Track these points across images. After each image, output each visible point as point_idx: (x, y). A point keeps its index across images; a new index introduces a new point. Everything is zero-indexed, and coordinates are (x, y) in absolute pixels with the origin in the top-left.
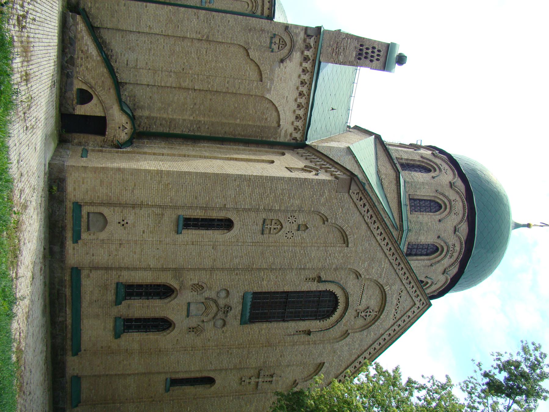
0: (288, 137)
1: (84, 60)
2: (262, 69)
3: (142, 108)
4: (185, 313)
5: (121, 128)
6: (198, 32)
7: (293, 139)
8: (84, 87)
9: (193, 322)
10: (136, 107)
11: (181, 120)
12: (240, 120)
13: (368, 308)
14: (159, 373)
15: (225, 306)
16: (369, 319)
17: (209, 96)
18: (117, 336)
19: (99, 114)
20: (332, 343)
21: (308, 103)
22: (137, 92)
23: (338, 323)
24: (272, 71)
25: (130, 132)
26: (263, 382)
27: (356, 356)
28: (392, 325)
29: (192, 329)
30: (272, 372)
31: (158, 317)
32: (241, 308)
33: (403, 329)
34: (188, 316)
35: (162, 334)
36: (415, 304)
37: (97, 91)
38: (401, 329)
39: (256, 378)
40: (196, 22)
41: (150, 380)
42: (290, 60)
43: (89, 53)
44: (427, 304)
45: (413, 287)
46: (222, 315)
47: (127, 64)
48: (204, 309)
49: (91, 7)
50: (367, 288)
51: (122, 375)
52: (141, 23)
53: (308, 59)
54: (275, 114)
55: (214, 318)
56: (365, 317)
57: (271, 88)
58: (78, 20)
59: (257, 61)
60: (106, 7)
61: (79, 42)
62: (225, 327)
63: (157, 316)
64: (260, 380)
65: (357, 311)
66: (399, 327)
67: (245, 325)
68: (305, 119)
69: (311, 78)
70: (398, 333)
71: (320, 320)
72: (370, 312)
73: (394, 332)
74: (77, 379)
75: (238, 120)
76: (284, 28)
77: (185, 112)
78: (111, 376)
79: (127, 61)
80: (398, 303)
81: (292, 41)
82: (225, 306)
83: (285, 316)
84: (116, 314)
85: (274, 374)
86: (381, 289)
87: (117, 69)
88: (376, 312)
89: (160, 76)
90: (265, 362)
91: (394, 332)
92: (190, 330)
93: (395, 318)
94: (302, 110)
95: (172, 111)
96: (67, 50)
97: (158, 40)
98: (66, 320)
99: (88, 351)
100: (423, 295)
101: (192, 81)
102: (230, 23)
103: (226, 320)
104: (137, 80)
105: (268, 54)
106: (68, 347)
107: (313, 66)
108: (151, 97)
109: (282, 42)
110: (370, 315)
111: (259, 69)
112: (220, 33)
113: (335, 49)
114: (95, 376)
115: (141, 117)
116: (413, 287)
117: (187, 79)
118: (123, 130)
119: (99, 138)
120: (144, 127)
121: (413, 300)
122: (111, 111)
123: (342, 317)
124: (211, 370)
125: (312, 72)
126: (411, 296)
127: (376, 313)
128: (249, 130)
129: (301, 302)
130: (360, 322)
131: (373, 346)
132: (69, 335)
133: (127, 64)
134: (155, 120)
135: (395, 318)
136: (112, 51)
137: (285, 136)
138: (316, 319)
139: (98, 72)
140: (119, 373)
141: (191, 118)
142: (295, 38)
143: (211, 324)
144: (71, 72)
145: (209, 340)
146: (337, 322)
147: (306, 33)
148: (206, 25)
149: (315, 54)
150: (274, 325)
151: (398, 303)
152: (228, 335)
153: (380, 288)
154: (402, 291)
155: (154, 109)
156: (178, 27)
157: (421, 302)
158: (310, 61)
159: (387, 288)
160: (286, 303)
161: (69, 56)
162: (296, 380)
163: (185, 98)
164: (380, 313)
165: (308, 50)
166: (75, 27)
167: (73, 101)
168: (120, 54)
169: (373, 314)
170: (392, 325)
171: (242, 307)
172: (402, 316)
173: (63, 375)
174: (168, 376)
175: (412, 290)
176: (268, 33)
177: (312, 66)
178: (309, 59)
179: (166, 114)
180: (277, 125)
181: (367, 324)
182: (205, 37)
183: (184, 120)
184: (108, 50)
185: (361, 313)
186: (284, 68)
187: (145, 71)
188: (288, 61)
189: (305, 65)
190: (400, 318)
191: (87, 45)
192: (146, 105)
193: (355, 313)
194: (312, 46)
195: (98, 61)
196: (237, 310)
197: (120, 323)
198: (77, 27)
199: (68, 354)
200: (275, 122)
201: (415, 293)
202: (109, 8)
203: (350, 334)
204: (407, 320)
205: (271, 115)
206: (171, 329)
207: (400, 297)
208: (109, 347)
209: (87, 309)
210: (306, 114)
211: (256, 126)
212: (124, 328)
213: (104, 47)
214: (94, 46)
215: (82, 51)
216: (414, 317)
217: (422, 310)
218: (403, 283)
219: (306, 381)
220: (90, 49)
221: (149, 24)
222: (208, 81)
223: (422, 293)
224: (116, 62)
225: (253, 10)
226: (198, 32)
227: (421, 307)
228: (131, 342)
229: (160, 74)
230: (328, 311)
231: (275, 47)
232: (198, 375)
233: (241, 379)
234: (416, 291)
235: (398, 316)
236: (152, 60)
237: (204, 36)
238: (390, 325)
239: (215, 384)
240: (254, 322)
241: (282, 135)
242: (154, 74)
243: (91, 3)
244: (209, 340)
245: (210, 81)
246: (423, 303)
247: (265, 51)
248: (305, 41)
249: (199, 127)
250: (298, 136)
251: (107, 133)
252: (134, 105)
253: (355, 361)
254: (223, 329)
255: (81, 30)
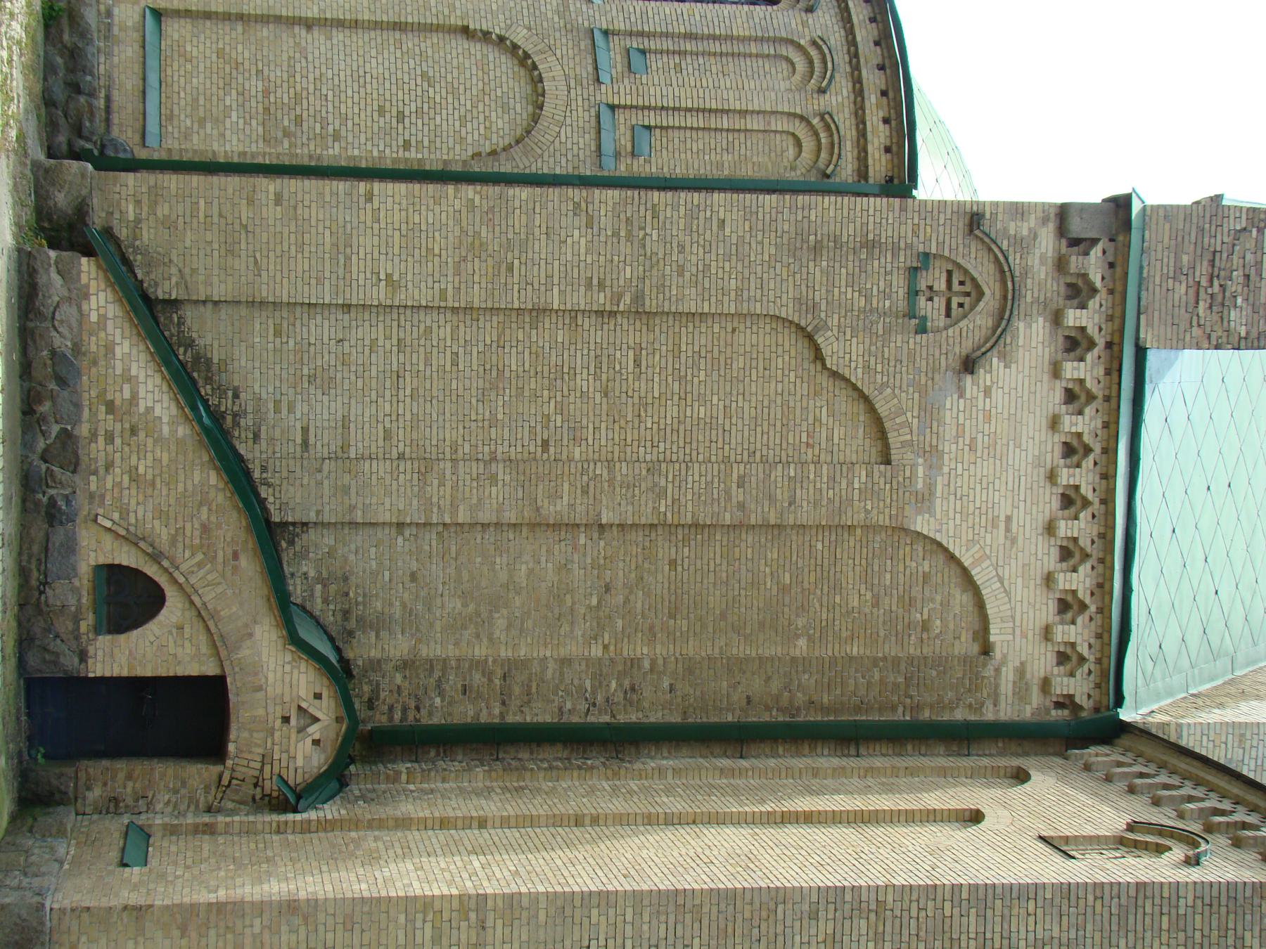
0: (1036, 698)
1: (118, 441)
2: (882, 409)
3: (380, 624)
5: (293, 721)
6: (595, 282)
7: (1059, 705)
8: (127, 557)
10: (352, 624)
11: (551, 665)
12: (810, 639)
17: (665, 550)
19: (193, 670)
21: (1106, 537)
22: (352, 557)
24: (930, 412)
25: (332, 735)
37: (184, 567)
40: (583, 241)
42: (1003, 356)
43: (142, 409)
47: (305, 443)
49: (138, 221)
52: (354, 269)
53: (1084, 344)
54: (961, 599)
57: (931, 487)
58: (84, 279)
59: (857, 377)
60: (202, 215)
61: (94, 370)
68: (1104, 610)
69: (1110, 426)
75: (802, 642)
76: (962, 224)
77: (566, 628)
79: (305, 430)
81: (1003, 272)
87: (264, 469)
89: (449, 484)
94: (1084, 569)
95: (509, 626)
96: (45, 407)
97: (429, 330)
101: (585, 492)
102: (728, 230)
104: (352, 508)
105: (903, 342)
107: (1114, 370)
108: (413, 577)
109: (961, 283)
111: (871, 409)
112: (687, 275)
113: (1204, 283)
115: (376, 665)
117: (566, 486)
118: (301, 730)
119: (198, 774)
120: (391, 708)
122: (245, 652)
125: (1112, 399)
128: (852, 682)
133: (305, 443)
134: (437, 674)
136: (236, 396)
137: (1021, 690)
139: (181, 487)
141: (596, 651)
142: (1015, 260)
144: (68, 502)
147: (1062, 231)
148: (625, 248)
149: (1116, 318)
155: (432, 625)
156: (510, 268)
158: (1096, 351)
161: (55, 429)
163: (564, 567)
165: (1083, 306)
166: (74, 310)
167: (77, 620)
168: (271, 406)
176: (895, 250)
177: (1108, 372)
178: (1092, 344)
179: (485, 640)
180: (975, 648)
182: (627, 299)
183: (565, 662)
184: (221, 390)
186: (981, 395)
187: (383, 468)
188: (995, 360)
189: (1072, 370)
191: (128, 378)
192: (397, 611)
194: (1098, 284)
195: (180, 442)
198: (85, 307)
200: (966, 637)
202: (216, 219)
205: (946, 604)
210: (1103, 587)
211: (885, 658)
213: (201, 383)
214: (158, 380)
215: (111, 407)
220: (142, 394)
221: (385, 267)
222: (655, 485)
224: (256, 437)
225: (821, 164)
226: (595, 282)
229: (448, 472)
231: (932, 310)
236: (408, 417)
237: (620, 296)
241: (1003, 689)
242: (423, 475)
243: (138, 203)
245: (663, 483)
247: (888, 331)
248: (1061, 265)
249: (633, 689)
250: (1079, 686)
251: (231, 747)
252: (346, 614)
255: (103, 318)
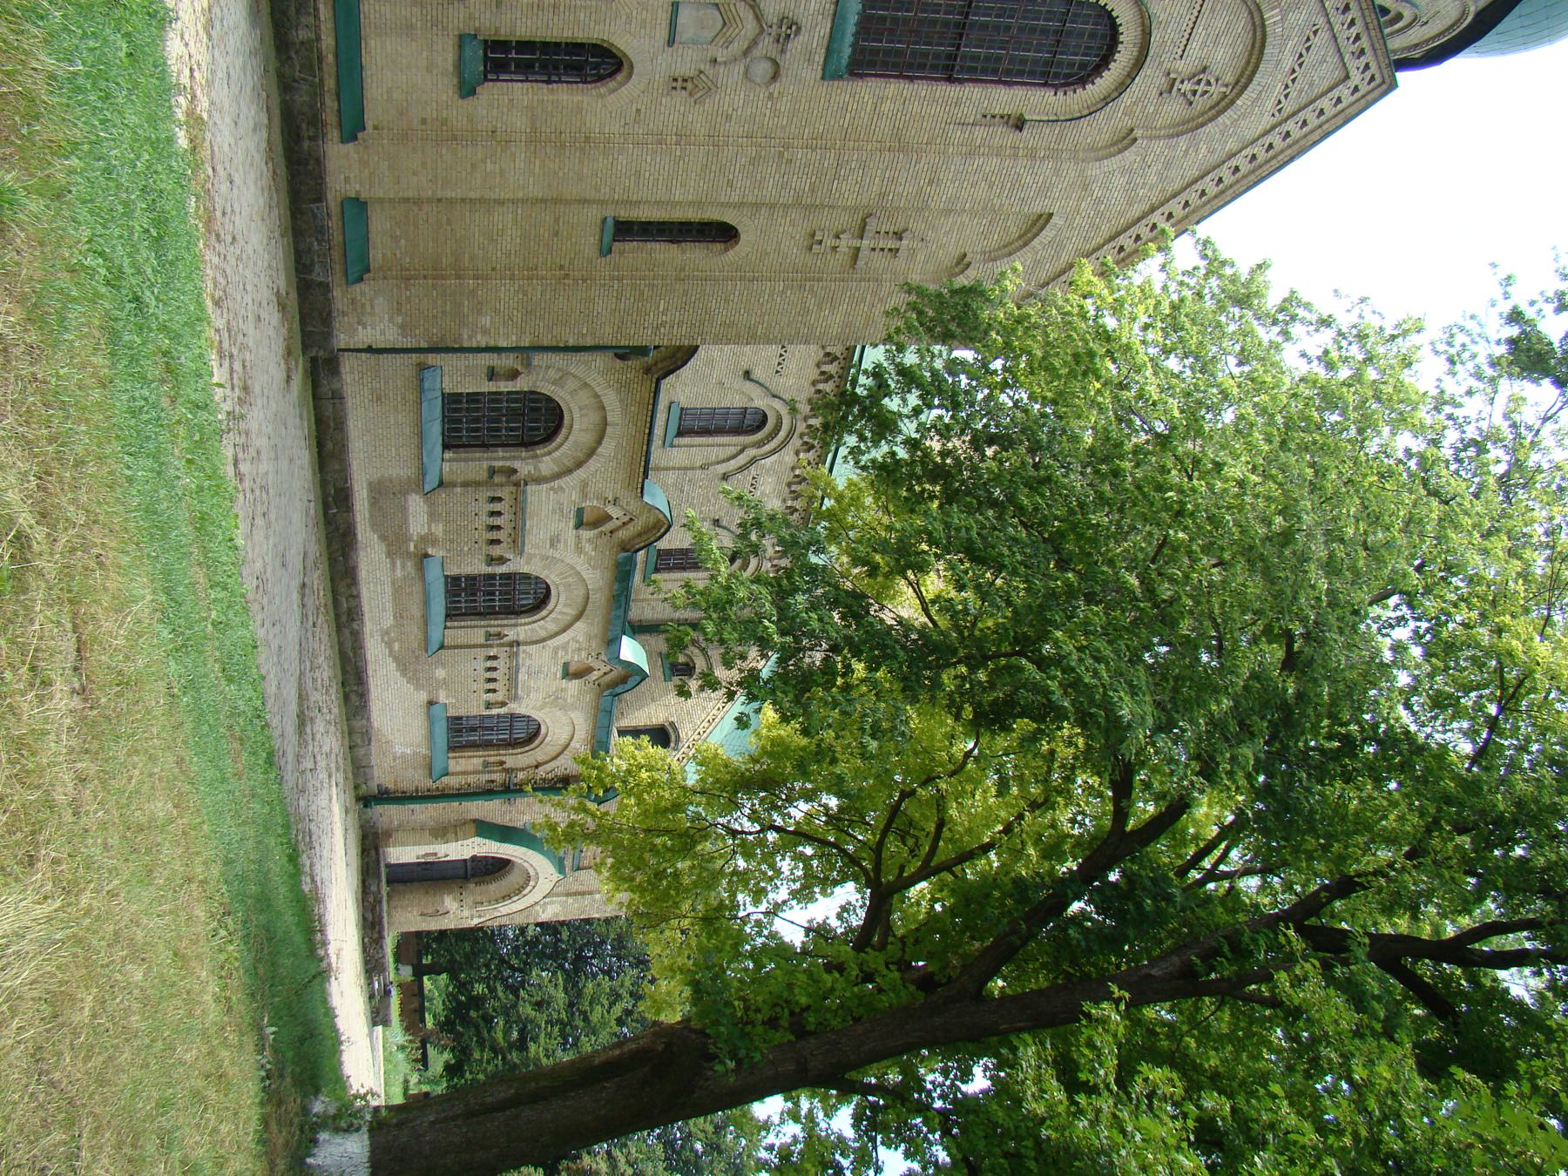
4: (662, 33)
9: (686, 61)
13: (1204, 70)
14: (584, 202)
15: (782, 21)
16: (1200, 103)
18: (467, 90)
20: (1083, 161)
23: (1107, 104)
26: (874, 249)
27: (1145, 207)
28: (1266, 133)
29: (680, 83)
30: (899, 227)
31: (584, 41)
32: (828, 30)
33: (1296, 147)
34: (671, 42)
35: (594, 93)
36: (1347, 77)
38: (1289, 146)
39: (853, 238)
41: (557, 220)
44: (1383, 82)
45: (1352, 23)
46: (770, 48)
48: (719, 24)
50: (1212, 10)
51: (481, 200)
55: (746, 53)
56: (1189, 96)
62: (778, 85)
63: (581, 36)
64: (865, 242)
65: (1169, 74)
66: (1284, 139)
67: (836, 83)
70: (1280, 158)
71: (1056, 88)
72: (1209, 83)
73: (1267, 151)
74: (358, 207)
78: (451, 201)
80: (1297, 68)
82: (782, 21)
83: (953, 66)
84: (461, 26)
85: (905, 230)
86: (1252, 18)
88: (1227, 86)
90: (882, 195)
91: (1267, 151)
92: (674, 84)
93: (1280, 111)
98: (318, 39)
99: (385, 131)
100: (1379, 52)
103: (782, 64)
106: (330, 117)
110: (1206, 92)
114: (406, 200)
116: (1352, 23)
121: (1344, 64)
123: (1122, 87)
124: (728, 205)
126: (1339, 51)
127: (1224, 89)
129: (1008, 28)
130: (1174, 109)
131: (1199, 186)
132: (330, 83)
135: (1280, 111)
138: (1045, 85)
140: (473, 195)
143: (738, 69)
145: (728, 118)
146: (1107, 100)
150: (921, 89)
151: (1297, 68)
152: (784, 105)
153: (1250, 13)
154: (1315, 33)
157: (1368, 75)
159: (1273, 16)
160: (963, 28)
162: (965, 255)
164: (1235, 91)
169: (1216, 90)
170: (1266, 133)
171: (831, 28)
172: (1300, 110)
173: (320, 198)
174: (610, 213)
175: (1347, 33)
181: (1193, 119)
185: (1182, 82)
190: (1294, 114)
193: (1162, 82)
196: (815, 35)
197: (475, 54)
199: (329, 137)
201: (1354, 43)
203: (1139, 141)
204: (1313, 122)
206: (620, 77)
207: (1308, 49)
208: (445, 122)
209: (377, 7)
212: (485, 66)
216: (1335, 116)
217: (1363, 96)
218: (1324, 6)
219: (994, 260)
223: (1377, 46)
227: (1364, 89)
228: (505, 110)
230: (1083, 66)
232: (692, 215)
233: (813, 235)
234: (1358, 38)
235: (1289, 107)
238: (1260, 129)
239: (737, 243)
240: (862, 76)
244: (728, 118)
246: (1372, 78)
253: (1139, 219)
254: (771, 88)
